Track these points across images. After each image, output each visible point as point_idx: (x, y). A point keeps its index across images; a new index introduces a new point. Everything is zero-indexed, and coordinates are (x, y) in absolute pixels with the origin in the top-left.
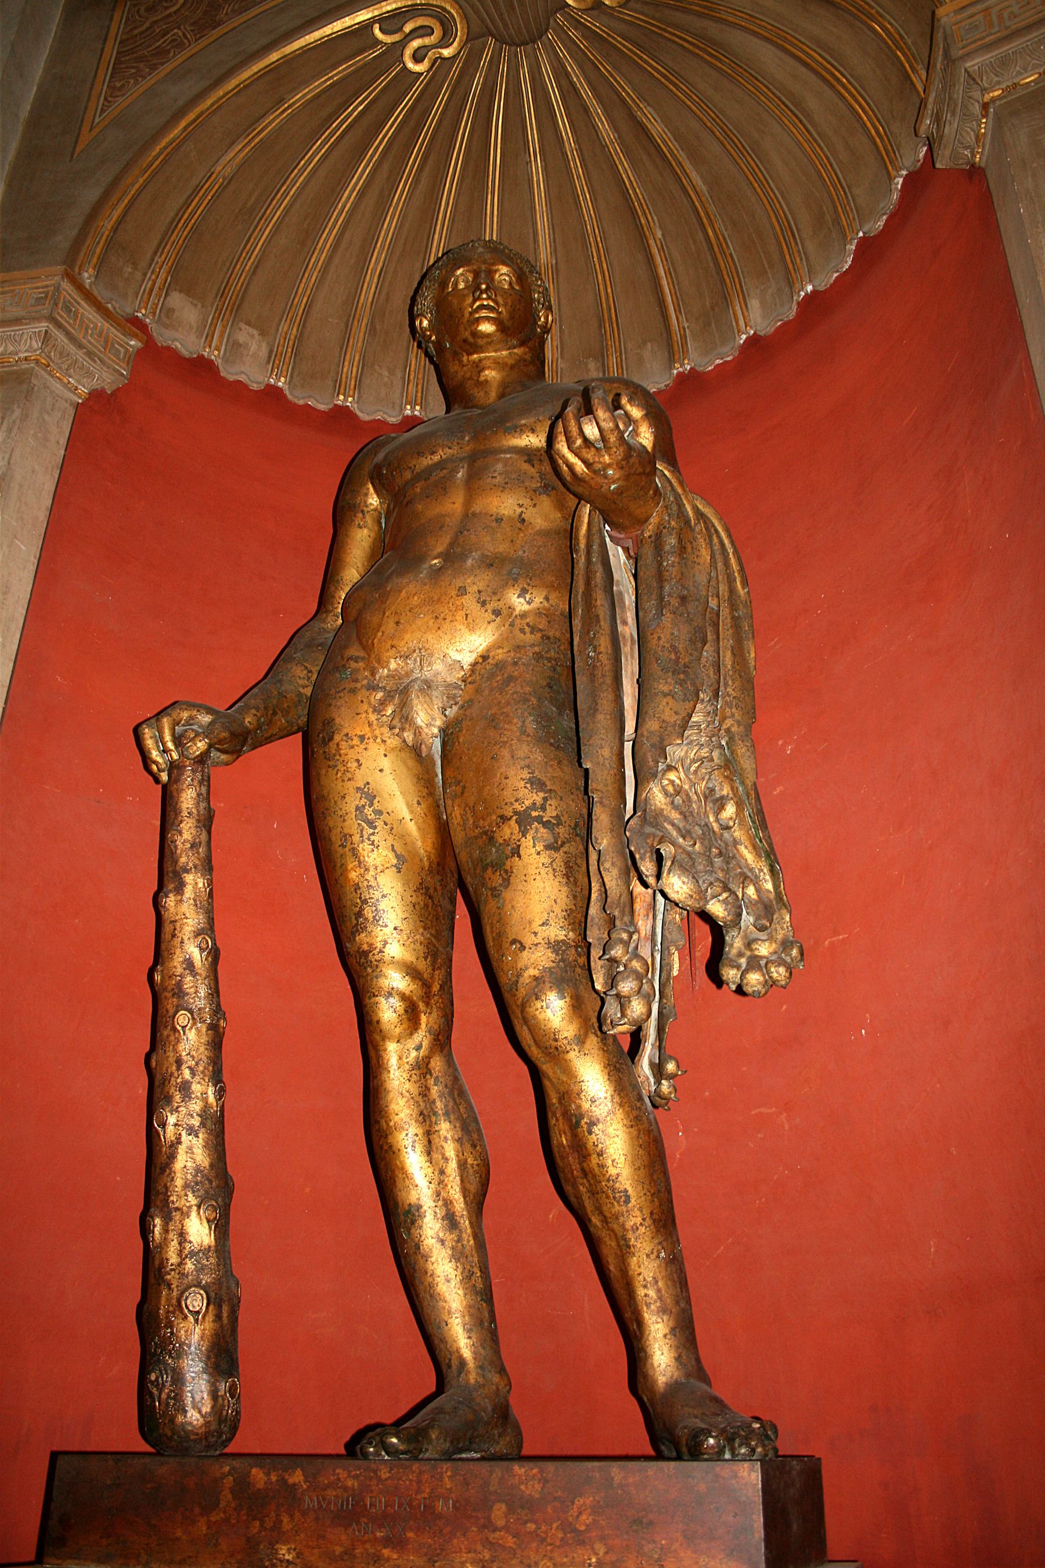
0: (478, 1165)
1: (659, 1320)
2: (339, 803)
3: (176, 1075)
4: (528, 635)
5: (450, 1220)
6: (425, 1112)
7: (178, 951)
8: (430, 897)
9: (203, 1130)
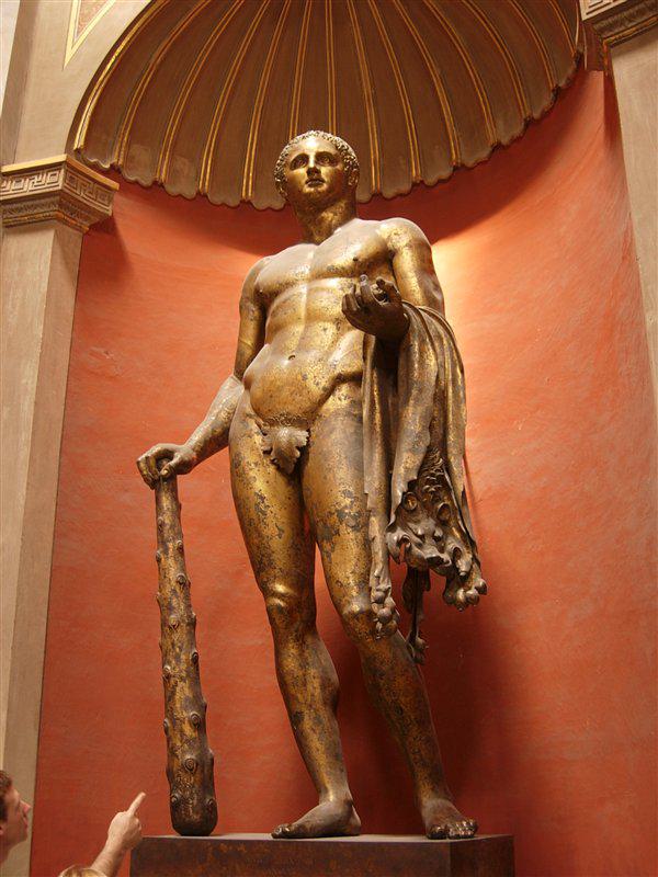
5: (318, 721)
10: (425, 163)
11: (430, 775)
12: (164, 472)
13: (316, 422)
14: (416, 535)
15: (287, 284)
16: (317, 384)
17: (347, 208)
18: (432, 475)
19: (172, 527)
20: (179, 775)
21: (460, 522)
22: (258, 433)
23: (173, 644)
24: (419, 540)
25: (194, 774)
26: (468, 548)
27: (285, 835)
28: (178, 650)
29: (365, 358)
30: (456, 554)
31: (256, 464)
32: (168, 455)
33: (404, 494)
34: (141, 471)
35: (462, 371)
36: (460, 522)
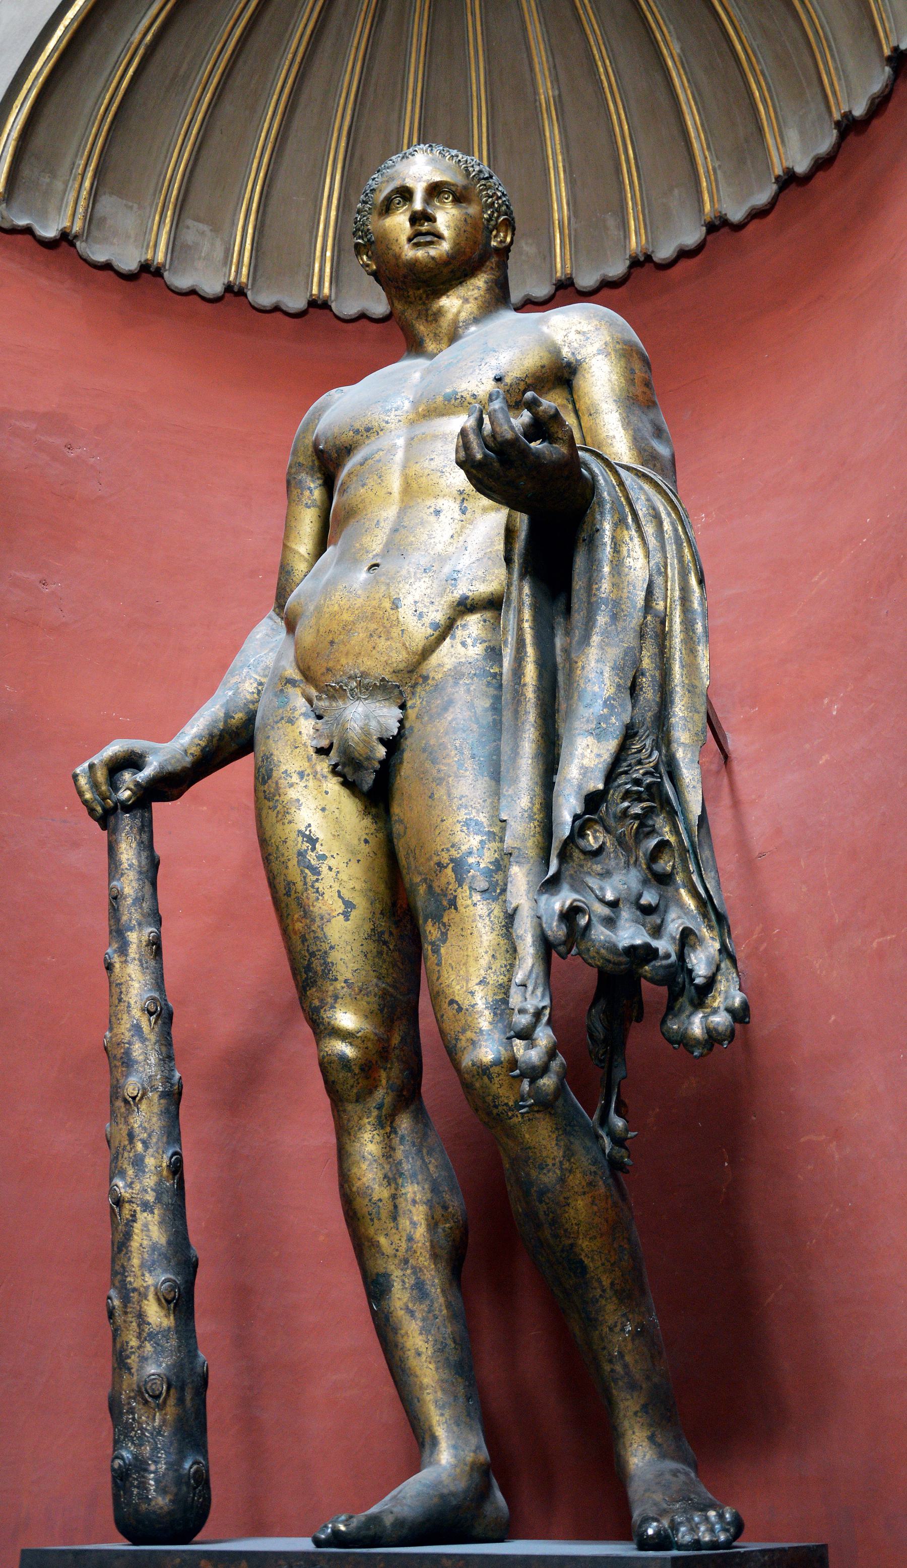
0: (451, 1228)
1: (628, 1397)
2: (281, 848)
3: (128, 1148)
4: (470, 648)
5: (420, 1290)
6: (390, 1175)
7: (125, 1017)
8: (385, 943)
9: (159, 1205)
10: (650, 226)
11: (645, 1407)
12: (125, 795)
13: (419, 689)
14: (602, 901)
15: (368, 430)
16: (421, 616)
17: (488, 290)
18: (637, 782)
19: (138, 901)
20: (132, 1411)
21: (695, 877)
22: (305, 715)
23: (131, 1136)
24: (606, 911)
25: (161, 1407)
26: (710, 927)
27: (337, 1539)
28: (139, 1146)
29: (508, 560)
30: (687, 938)
31: (301, 775)
32: (133, 761)
33: (576, 817)
34: (81, 794)
35: (701, 582)
36: (695, 877)
